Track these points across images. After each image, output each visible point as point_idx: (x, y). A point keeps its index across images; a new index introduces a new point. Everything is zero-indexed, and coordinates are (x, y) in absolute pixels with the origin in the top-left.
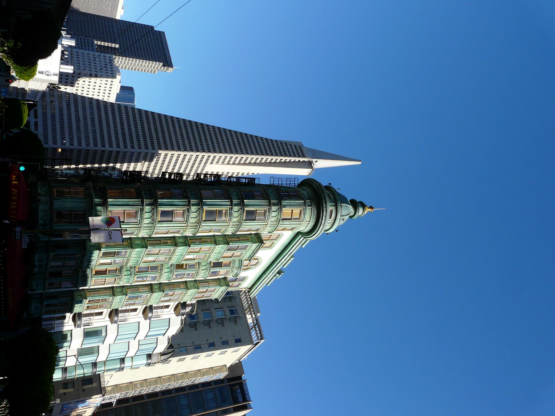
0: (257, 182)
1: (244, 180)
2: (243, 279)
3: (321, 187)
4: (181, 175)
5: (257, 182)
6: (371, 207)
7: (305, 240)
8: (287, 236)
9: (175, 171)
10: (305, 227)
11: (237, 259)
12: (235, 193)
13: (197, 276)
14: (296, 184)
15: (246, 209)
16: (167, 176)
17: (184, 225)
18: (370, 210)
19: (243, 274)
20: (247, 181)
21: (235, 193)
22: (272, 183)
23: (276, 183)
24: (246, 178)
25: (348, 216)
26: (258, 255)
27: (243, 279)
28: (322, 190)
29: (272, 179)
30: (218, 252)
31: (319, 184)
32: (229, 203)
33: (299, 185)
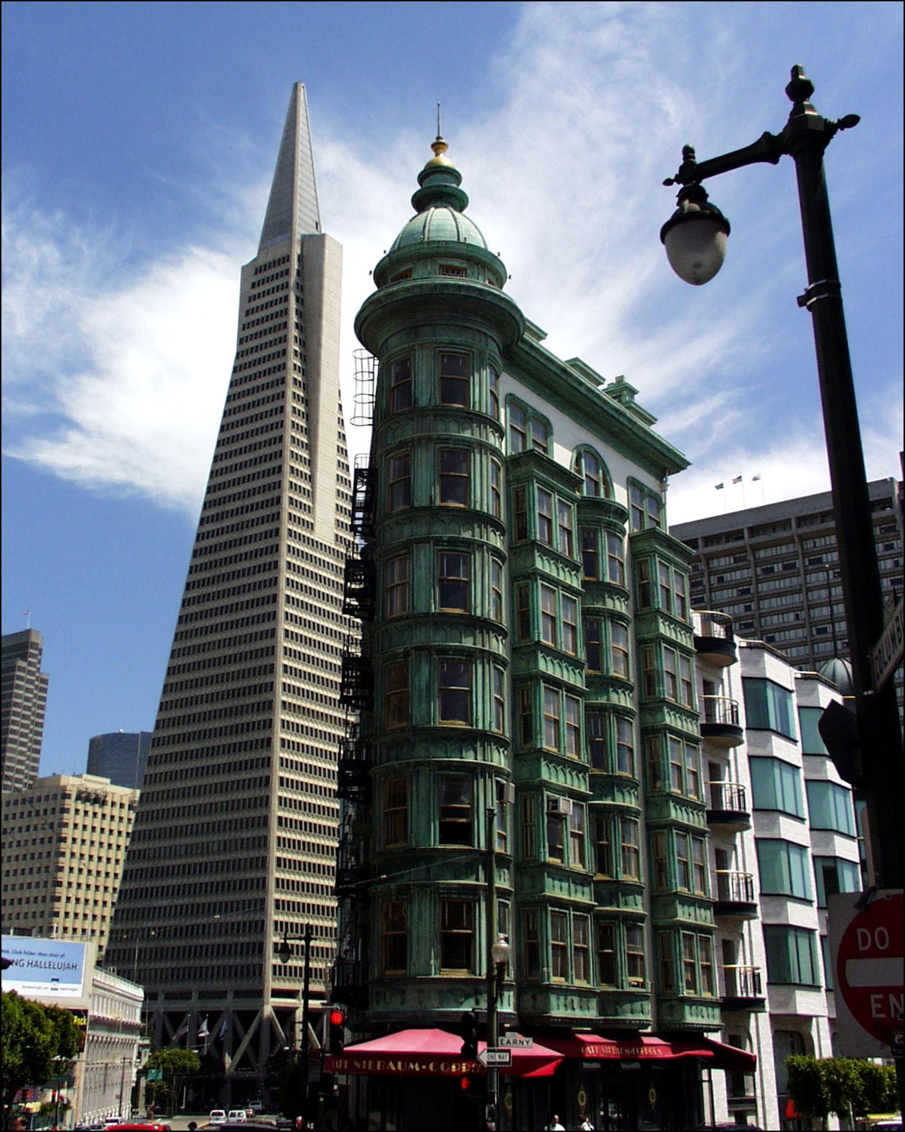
3: (378, 300)
12: (396, 531)
15: (438, 503)
21: (396, 531)
23: (368, 410)
29: (358, 421)
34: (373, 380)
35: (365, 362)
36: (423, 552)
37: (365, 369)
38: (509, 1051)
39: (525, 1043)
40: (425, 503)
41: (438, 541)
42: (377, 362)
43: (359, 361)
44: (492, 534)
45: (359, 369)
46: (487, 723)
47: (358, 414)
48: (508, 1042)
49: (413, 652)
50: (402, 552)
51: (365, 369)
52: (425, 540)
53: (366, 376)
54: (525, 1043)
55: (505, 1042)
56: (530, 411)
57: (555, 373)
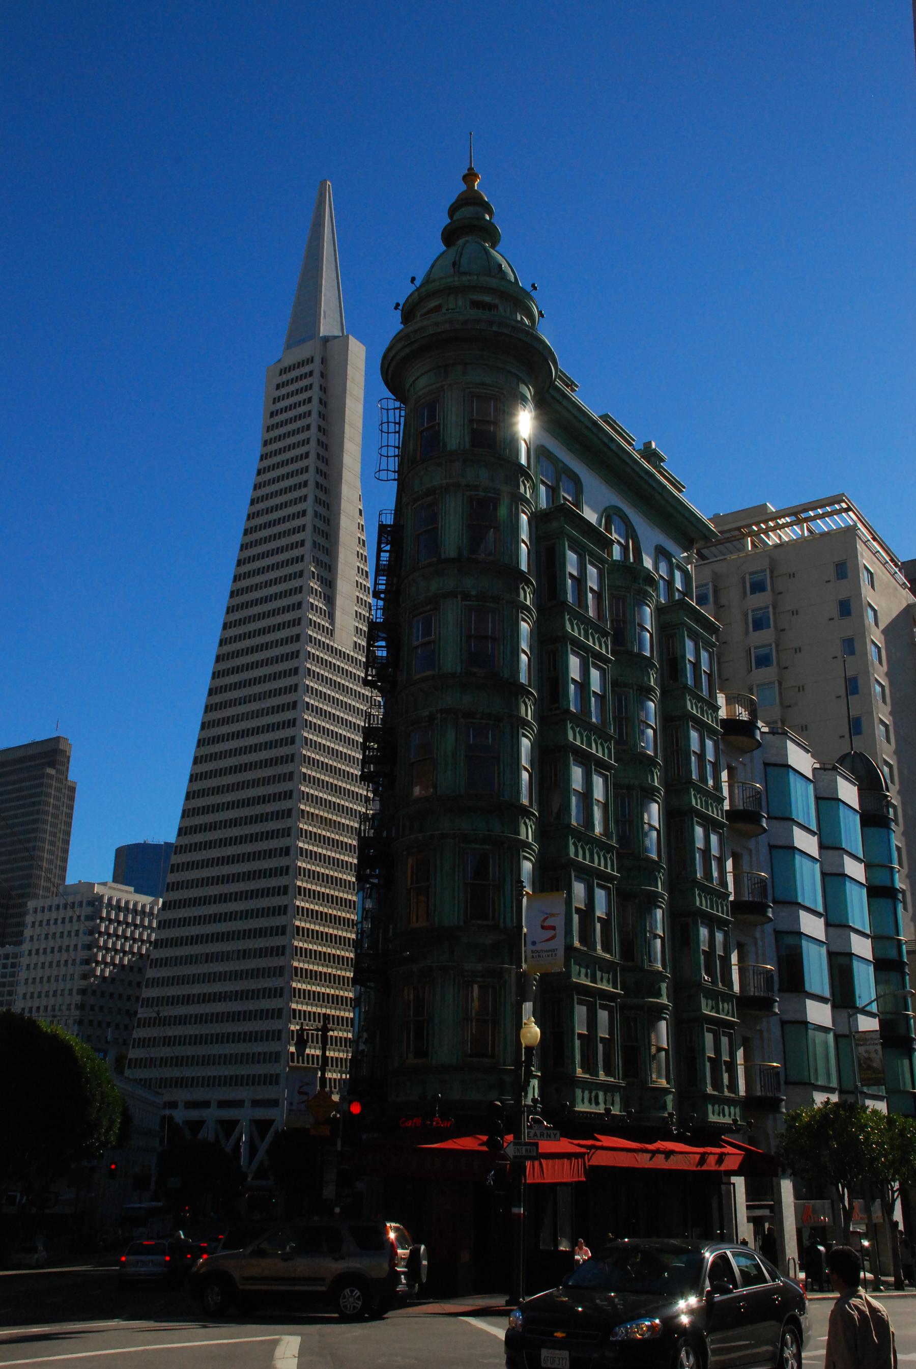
0: (389, 520)
1: (385, 556)
5: (389, 520)
14: (397, 404)
20: (388, 548)
22: (392, 476)
23: (393, 464)
24: (379, 550)
28: (415, 331)
29: (383, 475)
31: (397, 339)
34: (399, 432)
35: (391, 413)
37: (391, 419)
38: (536, 1145)
39: (552, 1136)
41: (466, 596)
42: (403, 413)
43: (385, 412)
45: (385, 420)
47: (384, 466)
48: (535, 1135)
49: (439, 715)
50: (428, 608)
51: (391, 419)
52: (452, 595)
53: (392, 428)
54: (552, 1136)
55: (532, 1135)
56: (560, 465)
57: (587, 427)
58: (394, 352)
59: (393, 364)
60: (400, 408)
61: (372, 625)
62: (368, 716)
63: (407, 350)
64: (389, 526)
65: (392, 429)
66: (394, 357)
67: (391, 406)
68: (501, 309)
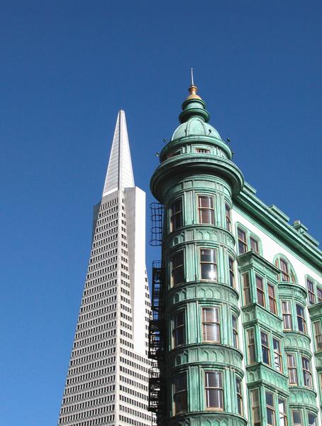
0: (159, 266)
1: (157, 286)
2: (310, 282)
4: (152, 381)
5: (159, 266)
6: (190, 90)
7: (244, 189)
8: (238, 217)
9: (146, 393)
10: (221, 190)
11: (278, 292)
13: (306, 353)
14: (160, 206)
16: (154, 404)
17: (228, 372)
18: (194, 93)
19: (302, 283)
20: (158, 281)
22: (159, 243)
24: (154, 283)
25: (205, 124)
26: (271, 260)
27: (310, 282)
29: (154, 243)
30: (267, 320)
31: (158, 170)
32: (192, 304)
33: (161, 203)
35: (157, 210)
36: (192, 307)
37: (157, 214)
40: (192, 279)
41: (201, 301)
42: (163, 210)
43: (153, 210)
44: (231, 298)
46: (234, 410)
52: (193, 301)
58: (155, 179)
59: (156, 183)
60: (161, 208)
61: (151, 322)
62: (151, 372)
63: (162, 177)
64: (158, 269)
65: (158, 219)
66: (157, 179)
67: (157, 206)
68: (211, 151)
